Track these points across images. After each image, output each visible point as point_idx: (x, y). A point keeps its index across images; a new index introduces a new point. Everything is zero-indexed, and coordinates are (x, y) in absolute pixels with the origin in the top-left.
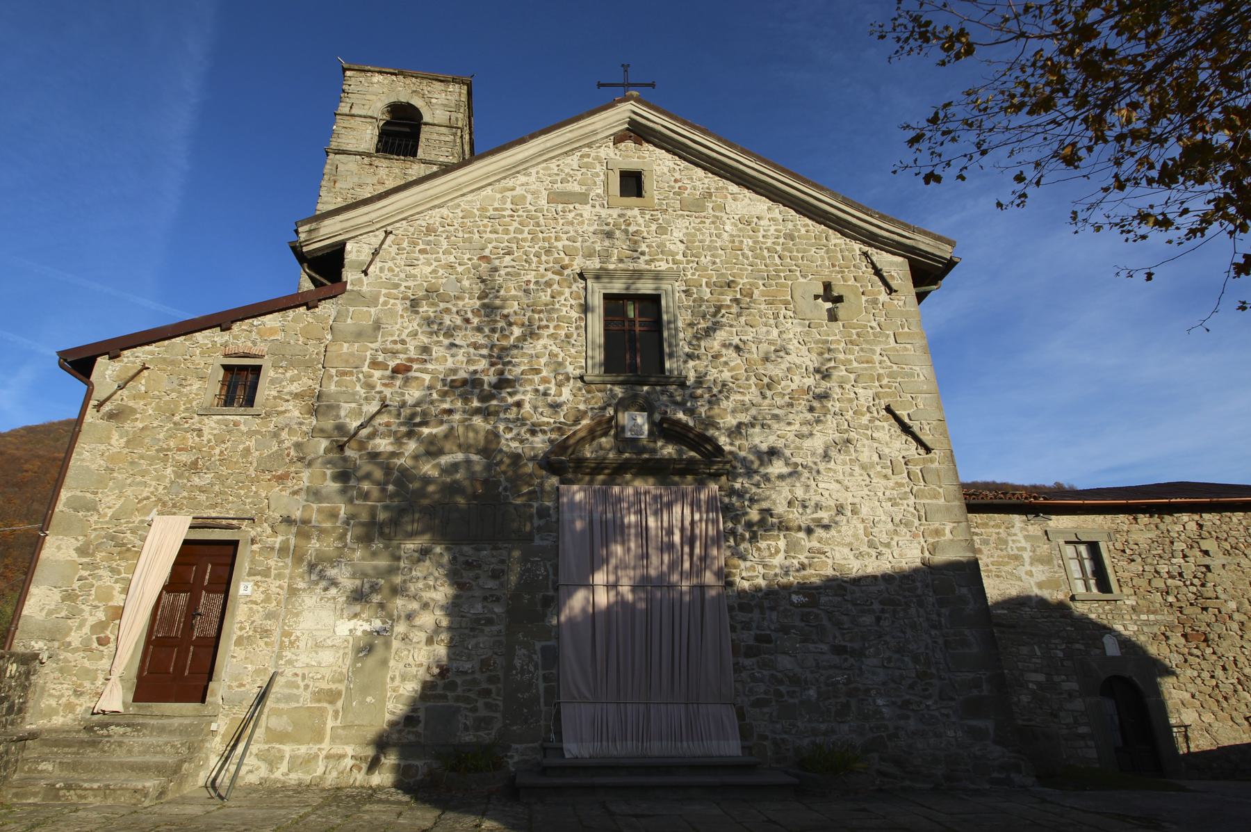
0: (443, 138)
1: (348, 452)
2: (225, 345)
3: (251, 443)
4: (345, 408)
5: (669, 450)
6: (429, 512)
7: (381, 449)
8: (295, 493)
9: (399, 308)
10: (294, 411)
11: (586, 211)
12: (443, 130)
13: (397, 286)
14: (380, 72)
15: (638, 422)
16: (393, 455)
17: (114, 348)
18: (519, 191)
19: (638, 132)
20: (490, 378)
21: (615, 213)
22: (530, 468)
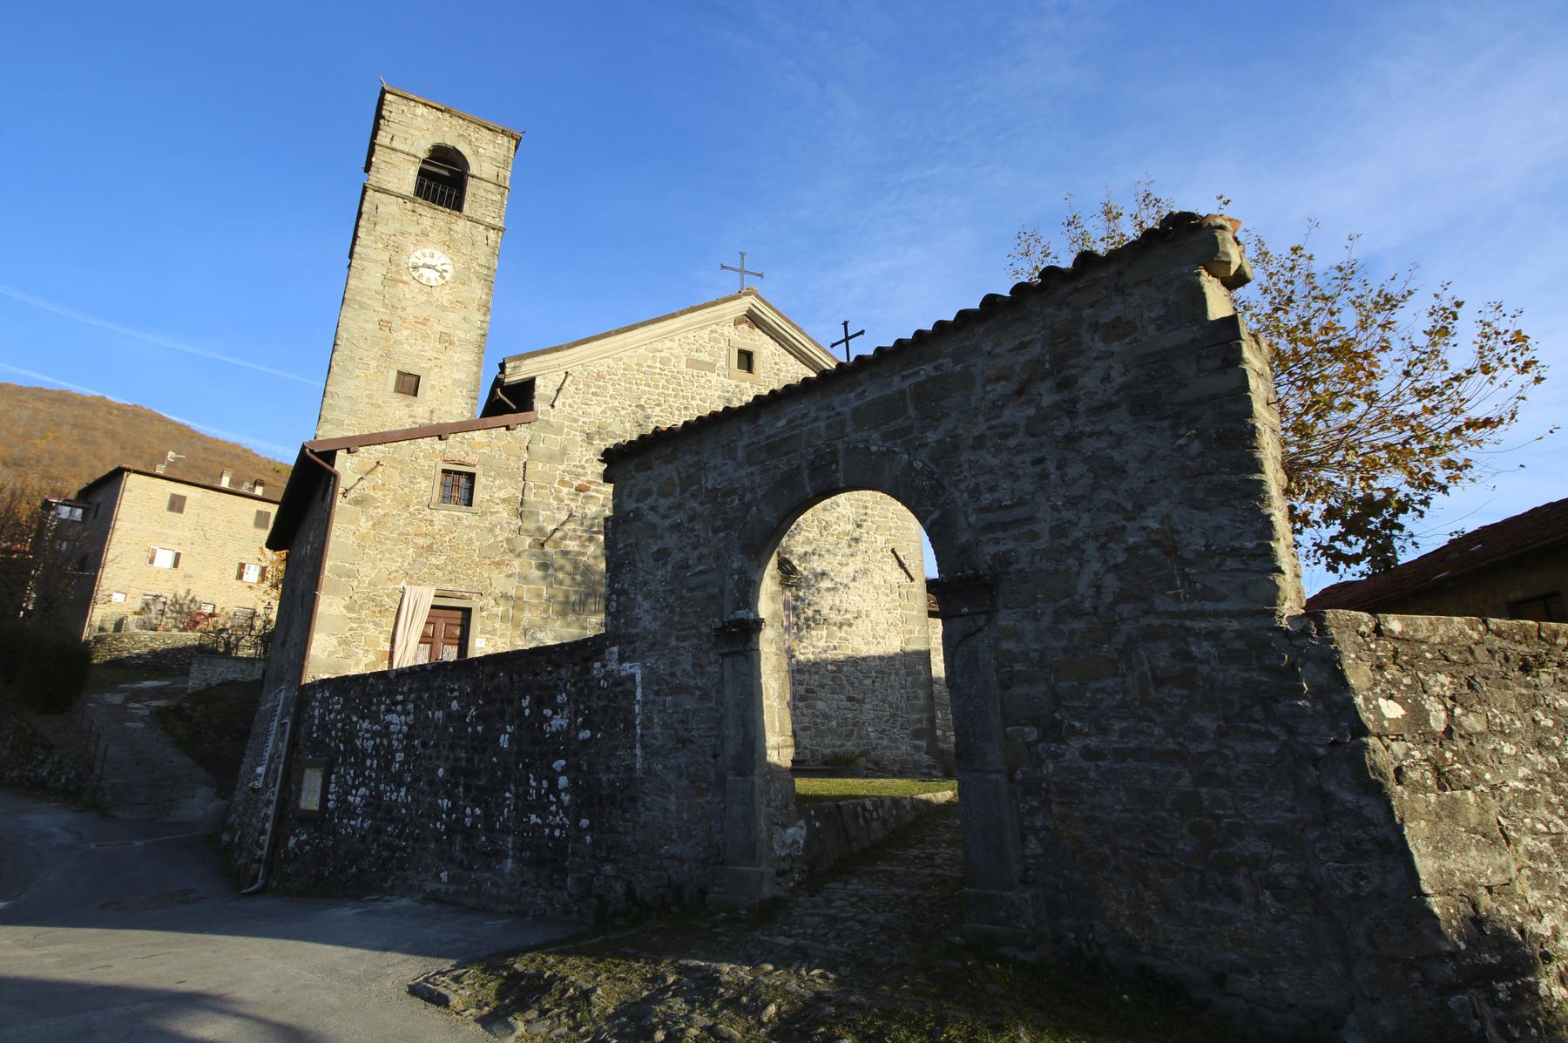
0: (490, 196)
1: (547, 548)
3: (473, 535)
4: (543, 514)
8: (510, 576)
9: (579, 439)
10: (504, 513)
11: (713, 377)
12: (491, 187)
13: (576, 421)
16: (579, 553)
18: (666, 354)
19: (753, 319)
21: (734, 382)
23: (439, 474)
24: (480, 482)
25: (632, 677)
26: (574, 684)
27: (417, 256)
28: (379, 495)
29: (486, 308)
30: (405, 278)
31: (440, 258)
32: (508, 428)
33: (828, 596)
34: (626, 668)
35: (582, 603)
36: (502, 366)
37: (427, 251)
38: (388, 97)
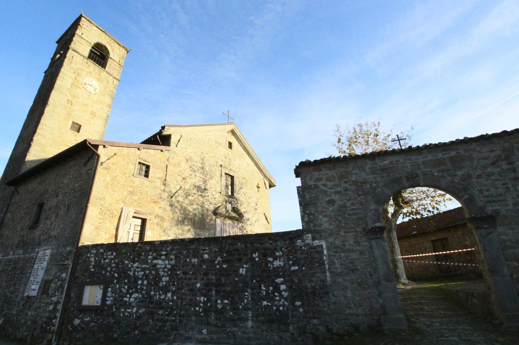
0: (116, 67)
2: (139, 155)
4: (172, 185)
5: (234, 215)
6: (191, 219)
7: (180, 200)
8: (161, 208)
10: (159, 184)
11: (221, 148)
13: (183, 153)
15: (229, 207)
16: (183, 202)
17: (113, 145)
19: (233, 132)
20: (203, 187)
22: (210, 213)
23: (137, 163)
25: (321, 246)
26: (286, 248)
27: (86, 80)
28: (114, 167)
30: (80, 87)
31: (95, 84)
32: (162, 151)
33: (249, 226)
34: (317, 243)
35: (183, 221)
36: (163, 128)
37: (91, 79)
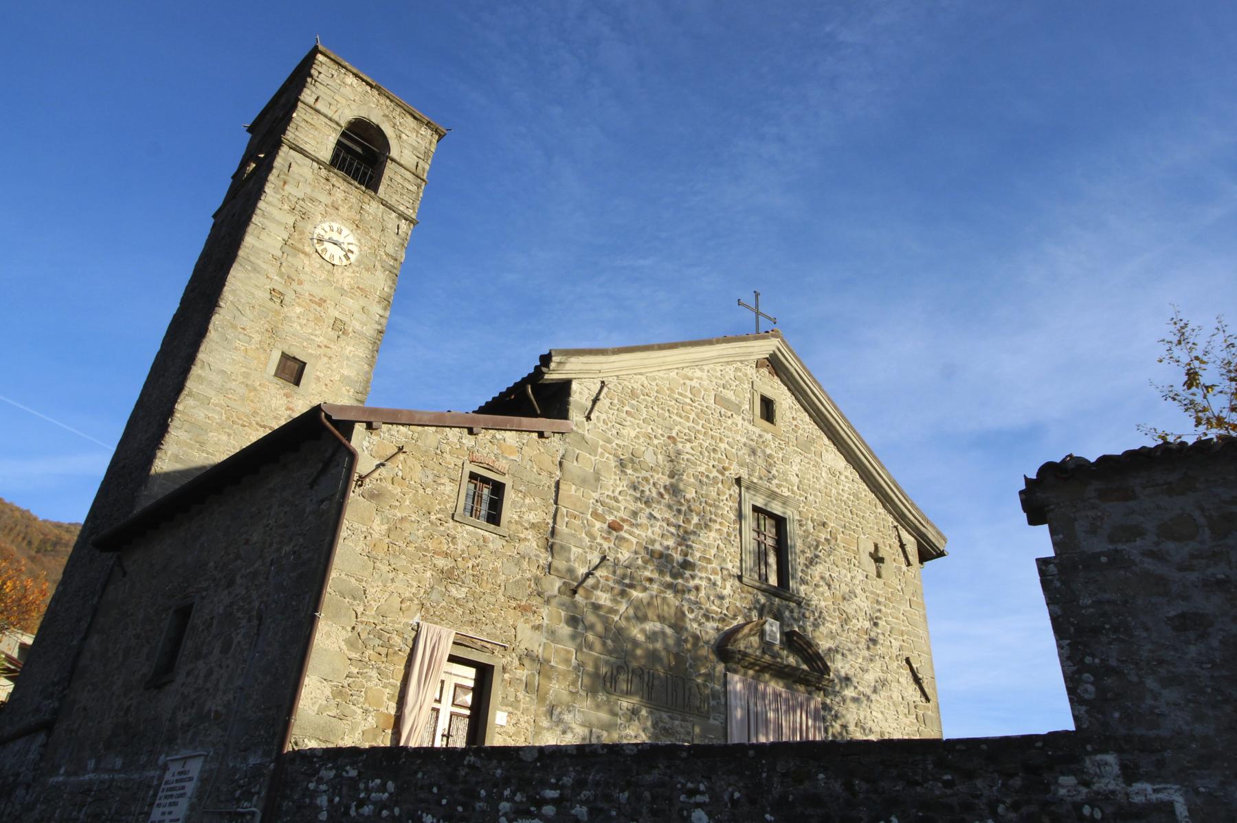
0: (406, 184)
1: (578, 598)
2: (471, 451)
3: (498, 564)
5: (792, 660)
6: (639, 673)
7: (602, 602)
8: (537, 628)
9: (613, 464)
10: (532, 543)
12: (408, 175)
13: (609, 441)
14: (356, 75)
15: (773, 628)
16: (612, 611)
18: (694, 383)
19: (775, 364)
20: (678, 557)
21: (758, 431)
22: (704, 651)
23: (466, 478)
24: (509, 496)
25: (1168, 807)
26: (1015, 807)
27: (324, 228)
28: (397, 490)
29: (386, 302)
30: (307, 249)
31: (348, 237)
32: (541, 435)
33: (852, 706)
34: (1144, 791)
35: (613, 679)
36: (546, 360)
37: (335, 226)
38: (320, 57)
